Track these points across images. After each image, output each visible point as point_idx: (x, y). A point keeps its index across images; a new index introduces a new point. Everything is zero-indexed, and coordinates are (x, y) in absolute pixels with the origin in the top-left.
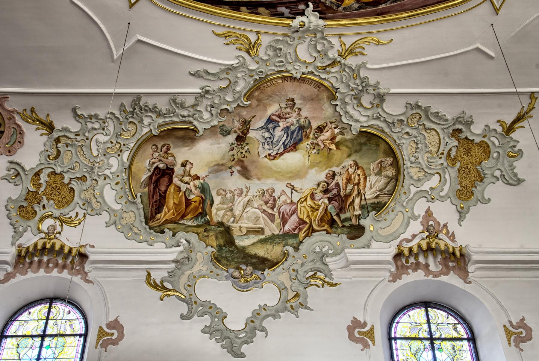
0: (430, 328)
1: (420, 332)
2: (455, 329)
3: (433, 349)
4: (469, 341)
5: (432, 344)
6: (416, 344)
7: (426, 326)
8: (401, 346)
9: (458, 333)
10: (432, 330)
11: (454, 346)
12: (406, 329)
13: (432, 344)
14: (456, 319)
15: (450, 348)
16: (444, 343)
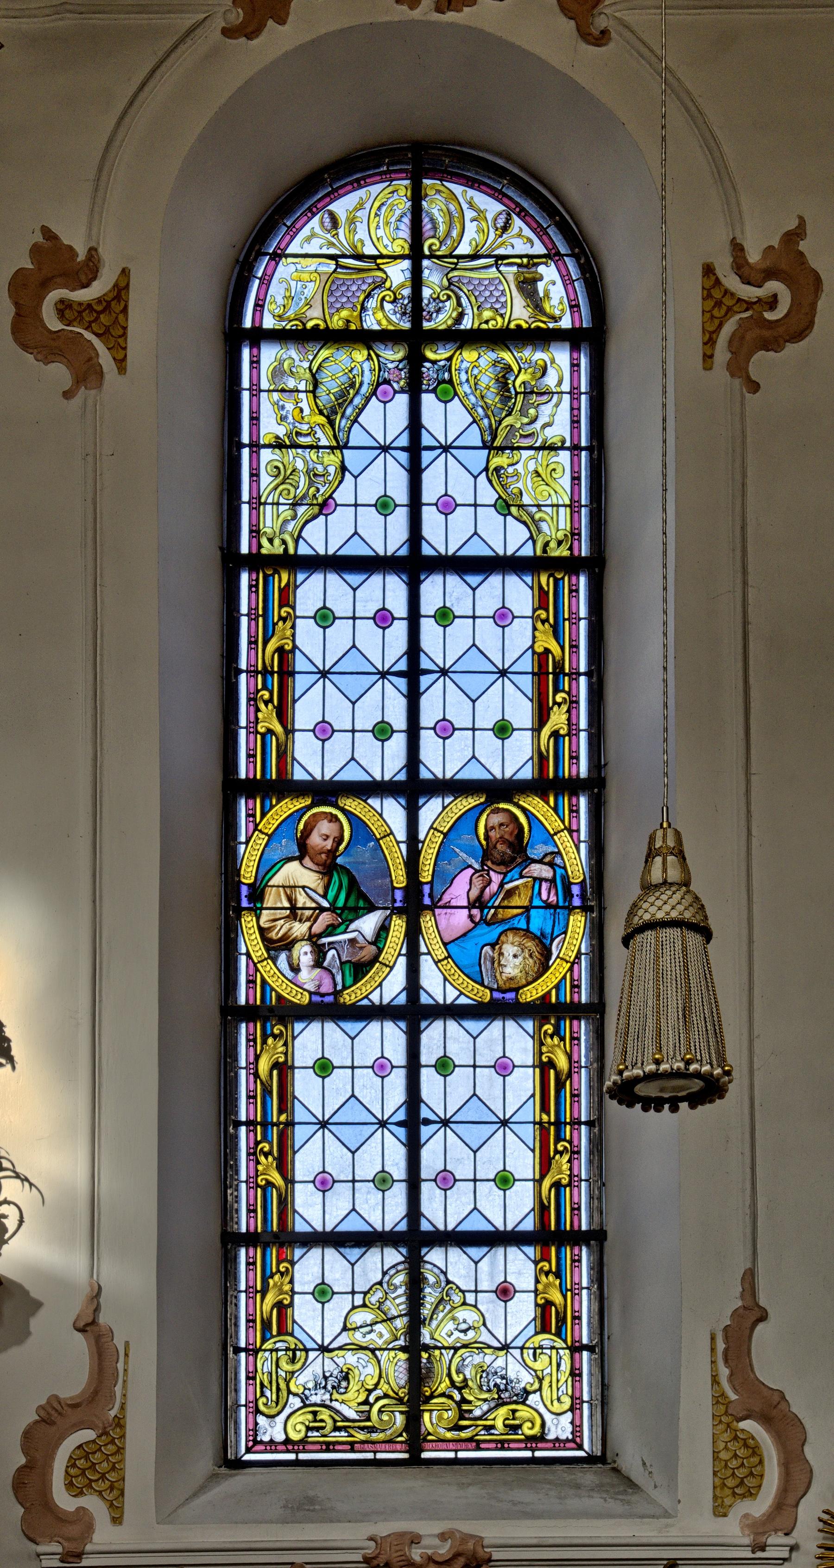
0: (417, 280)
1: (372, 303)
2: (528, 286)
3: (414, 390)
4: (575, 348)
5: (415, 361)
6: (343, 364)
7: (398, 273)
8: (278, 372)
9: (536, 302)
10: (426, 293)
11: (508, 369)
12: (311, 289)
13: (415, 361)
14: (541, 232)
15: (487, 380)
16: (469, 355)
